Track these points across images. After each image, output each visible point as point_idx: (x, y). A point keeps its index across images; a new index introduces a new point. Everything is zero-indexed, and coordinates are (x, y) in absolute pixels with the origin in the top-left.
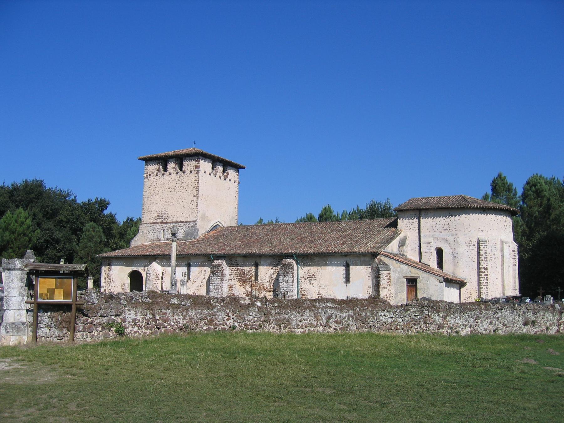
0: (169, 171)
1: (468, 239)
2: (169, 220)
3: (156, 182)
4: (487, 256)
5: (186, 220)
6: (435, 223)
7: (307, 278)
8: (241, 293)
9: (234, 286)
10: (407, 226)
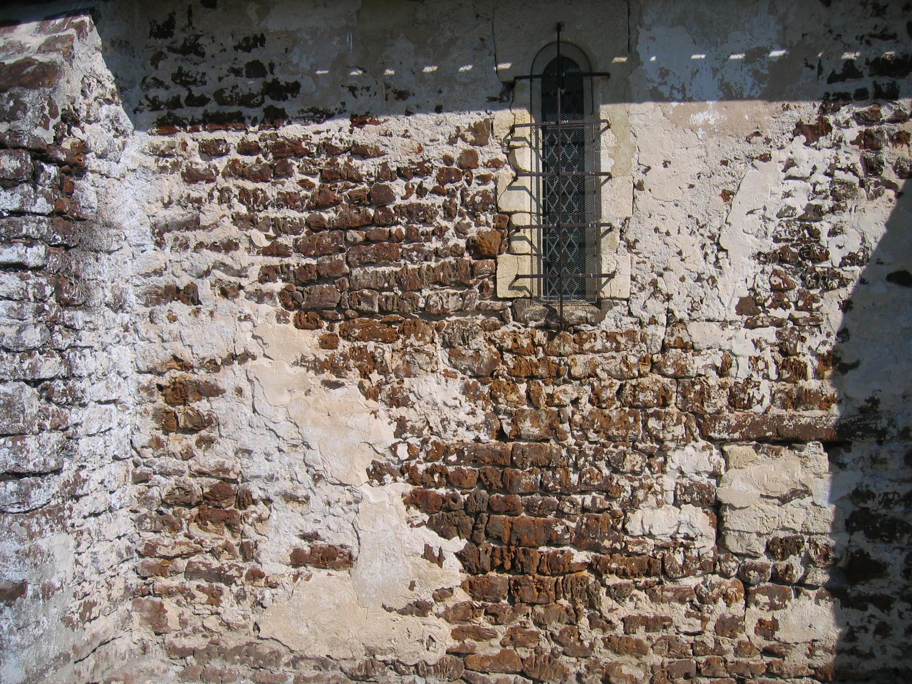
8: (335, 467)
9: (227, 378)
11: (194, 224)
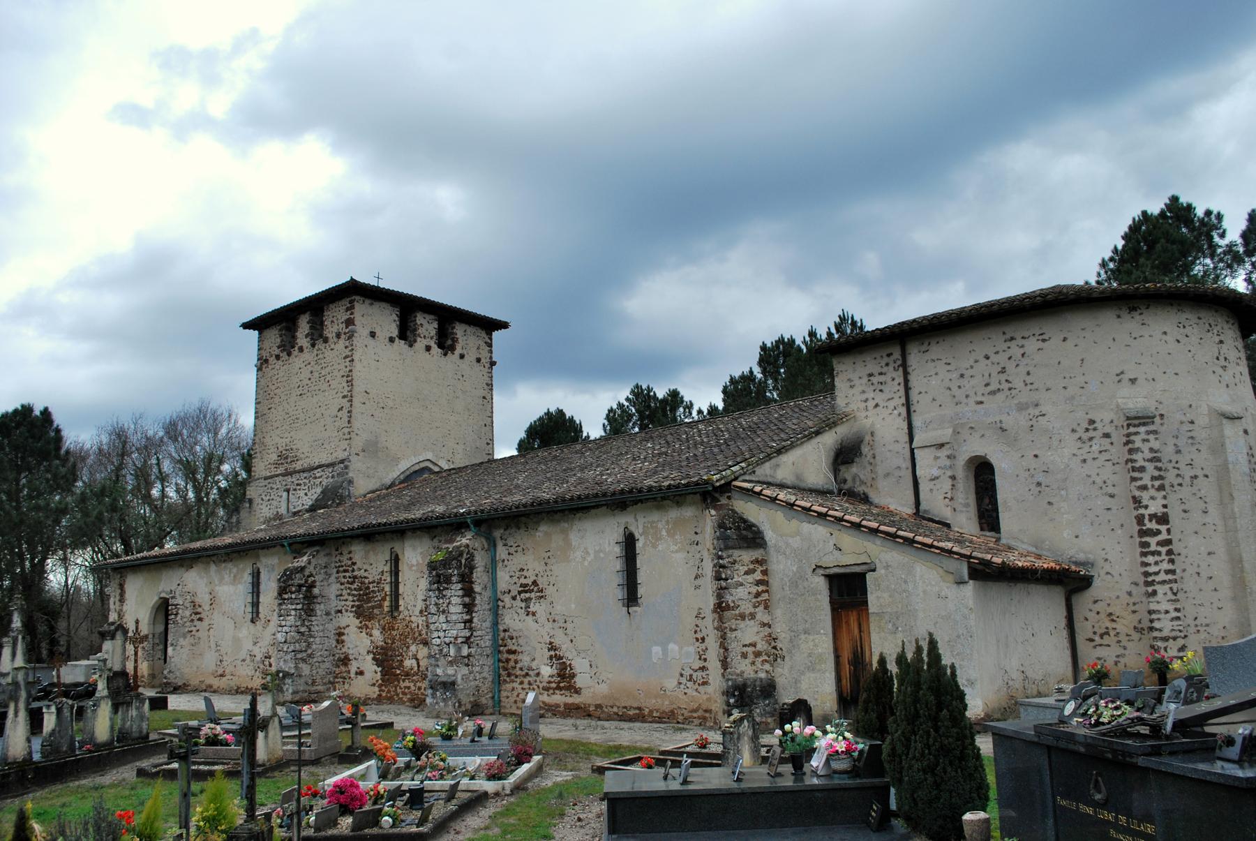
0: (300, 345)
1: (1081, 417)
2: (298, 466)
4: (1160, 469)
5: (329, 461)
6: (955, 375)
7: (520, 593)
8: (361, 651)
9: (346, 631)
10: (864, 397)
11: (341, 595)
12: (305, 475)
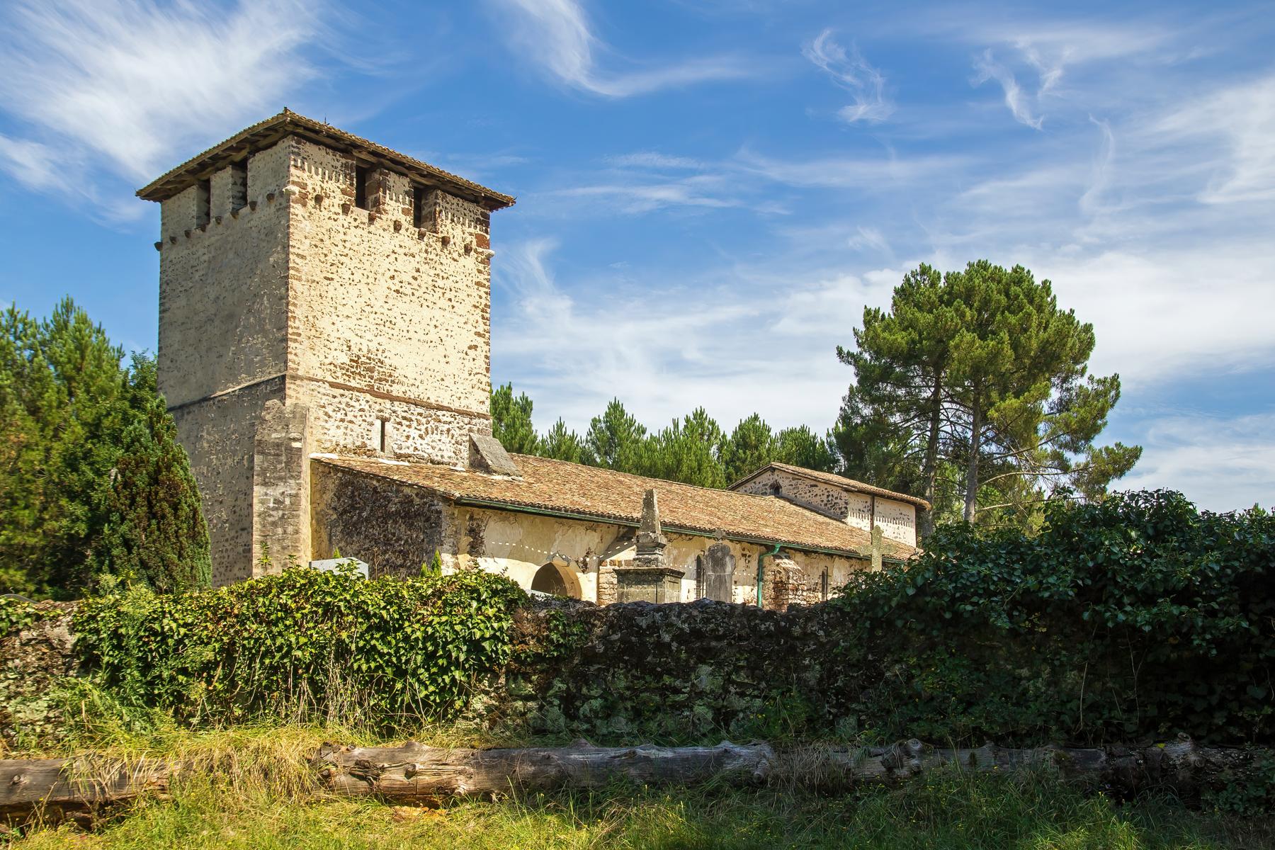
2: (397, 390)
3: (342, 236)
12: (419, 410)
